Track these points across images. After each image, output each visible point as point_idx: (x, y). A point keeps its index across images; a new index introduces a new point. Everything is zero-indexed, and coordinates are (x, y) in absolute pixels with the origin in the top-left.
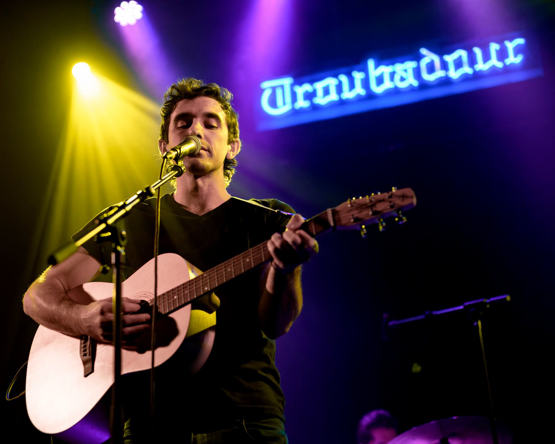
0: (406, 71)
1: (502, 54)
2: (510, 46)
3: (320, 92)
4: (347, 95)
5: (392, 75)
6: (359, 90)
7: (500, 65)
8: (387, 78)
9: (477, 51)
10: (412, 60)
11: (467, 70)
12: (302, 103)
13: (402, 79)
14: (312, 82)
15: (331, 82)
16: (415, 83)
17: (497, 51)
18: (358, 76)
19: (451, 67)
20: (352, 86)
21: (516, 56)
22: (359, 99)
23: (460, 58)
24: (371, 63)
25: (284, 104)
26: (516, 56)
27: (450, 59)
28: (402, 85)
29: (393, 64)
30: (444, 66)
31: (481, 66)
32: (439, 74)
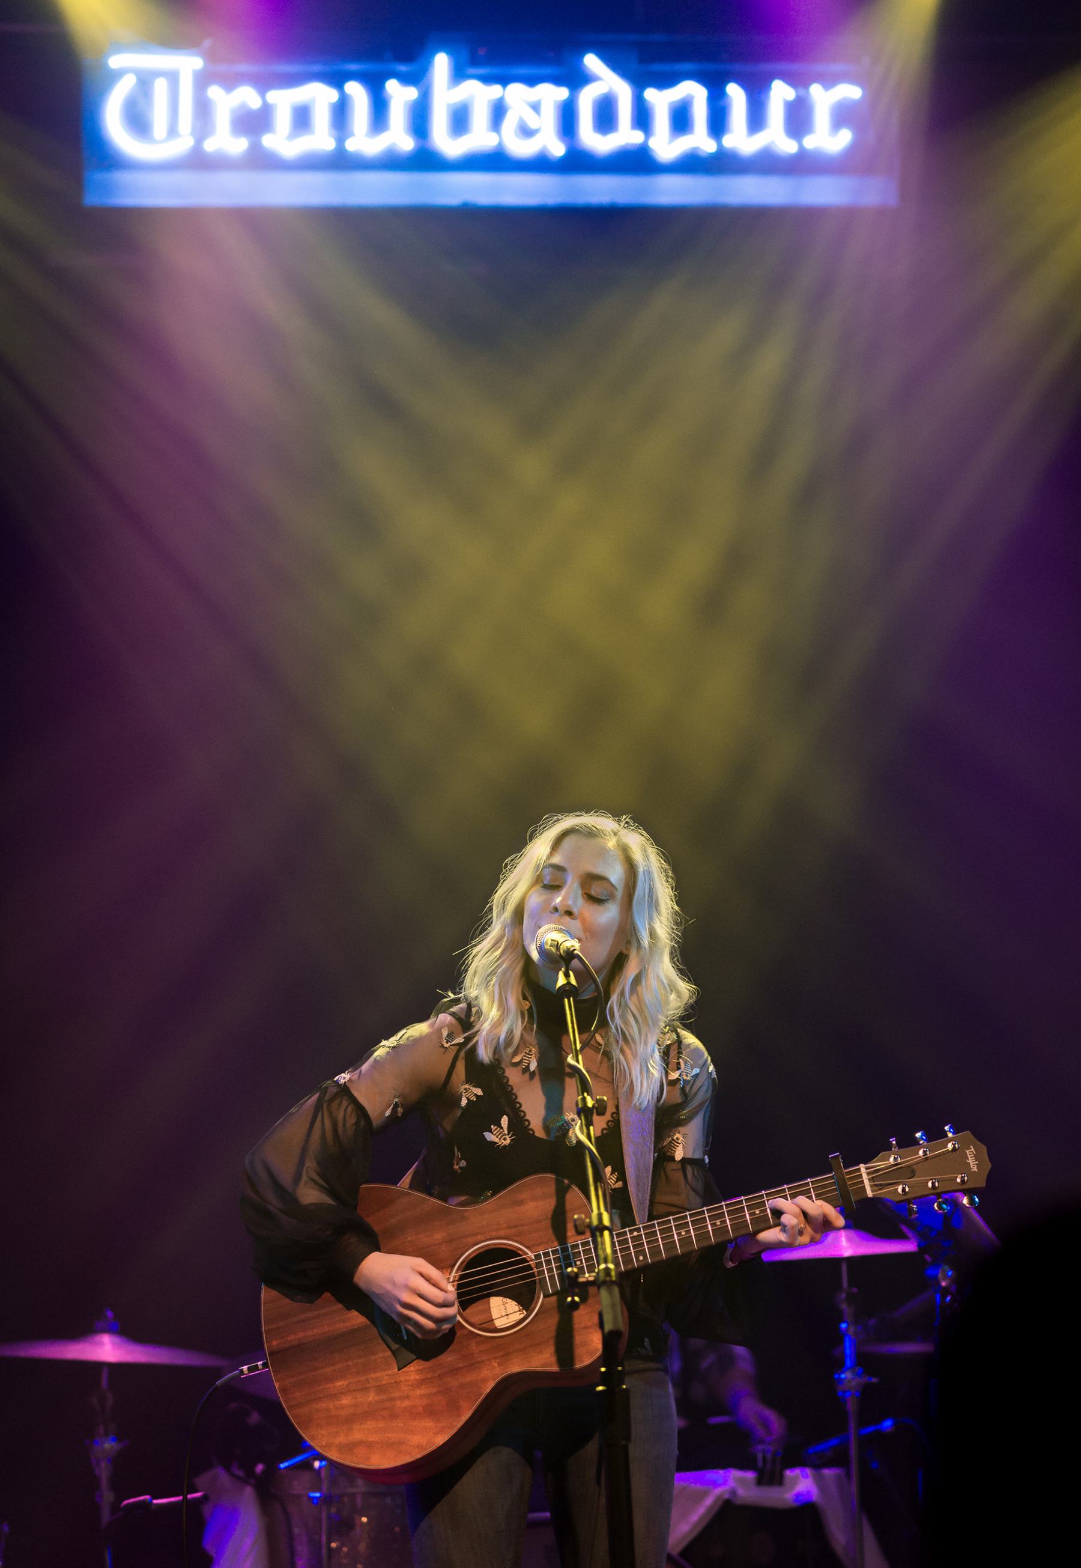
0: (536, 107)
3: (283, 119)
5: (498, 112)
8: (480, 117)
9: (735, 92)
10: (558, 81)
13: (526, 132)
14: (263, 84)
22: (392, 162)
24: (441, 63)
25: (173, 131)
27: (660, 99)
28: (521, 148)
29: (504, 81)
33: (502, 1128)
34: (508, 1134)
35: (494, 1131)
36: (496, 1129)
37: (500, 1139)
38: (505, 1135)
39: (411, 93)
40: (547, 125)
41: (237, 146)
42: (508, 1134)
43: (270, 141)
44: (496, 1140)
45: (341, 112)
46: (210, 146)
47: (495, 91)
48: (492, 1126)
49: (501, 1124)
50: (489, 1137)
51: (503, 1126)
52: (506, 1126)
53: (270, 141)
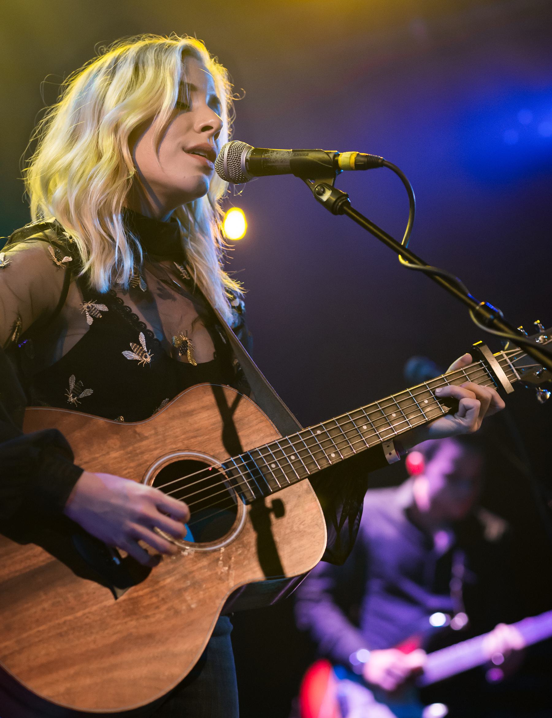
33: (141, 345)
34: (148, 352)
35: (134, 349)
36: (135, 347)
37: (141, 357)
38: (145, 352)
42: (148, 352)
44: (137, 357)
48: (131, 344)
49: (139, 342)
50: (129, 355)
51: (141, 342)
52: (145, 344)
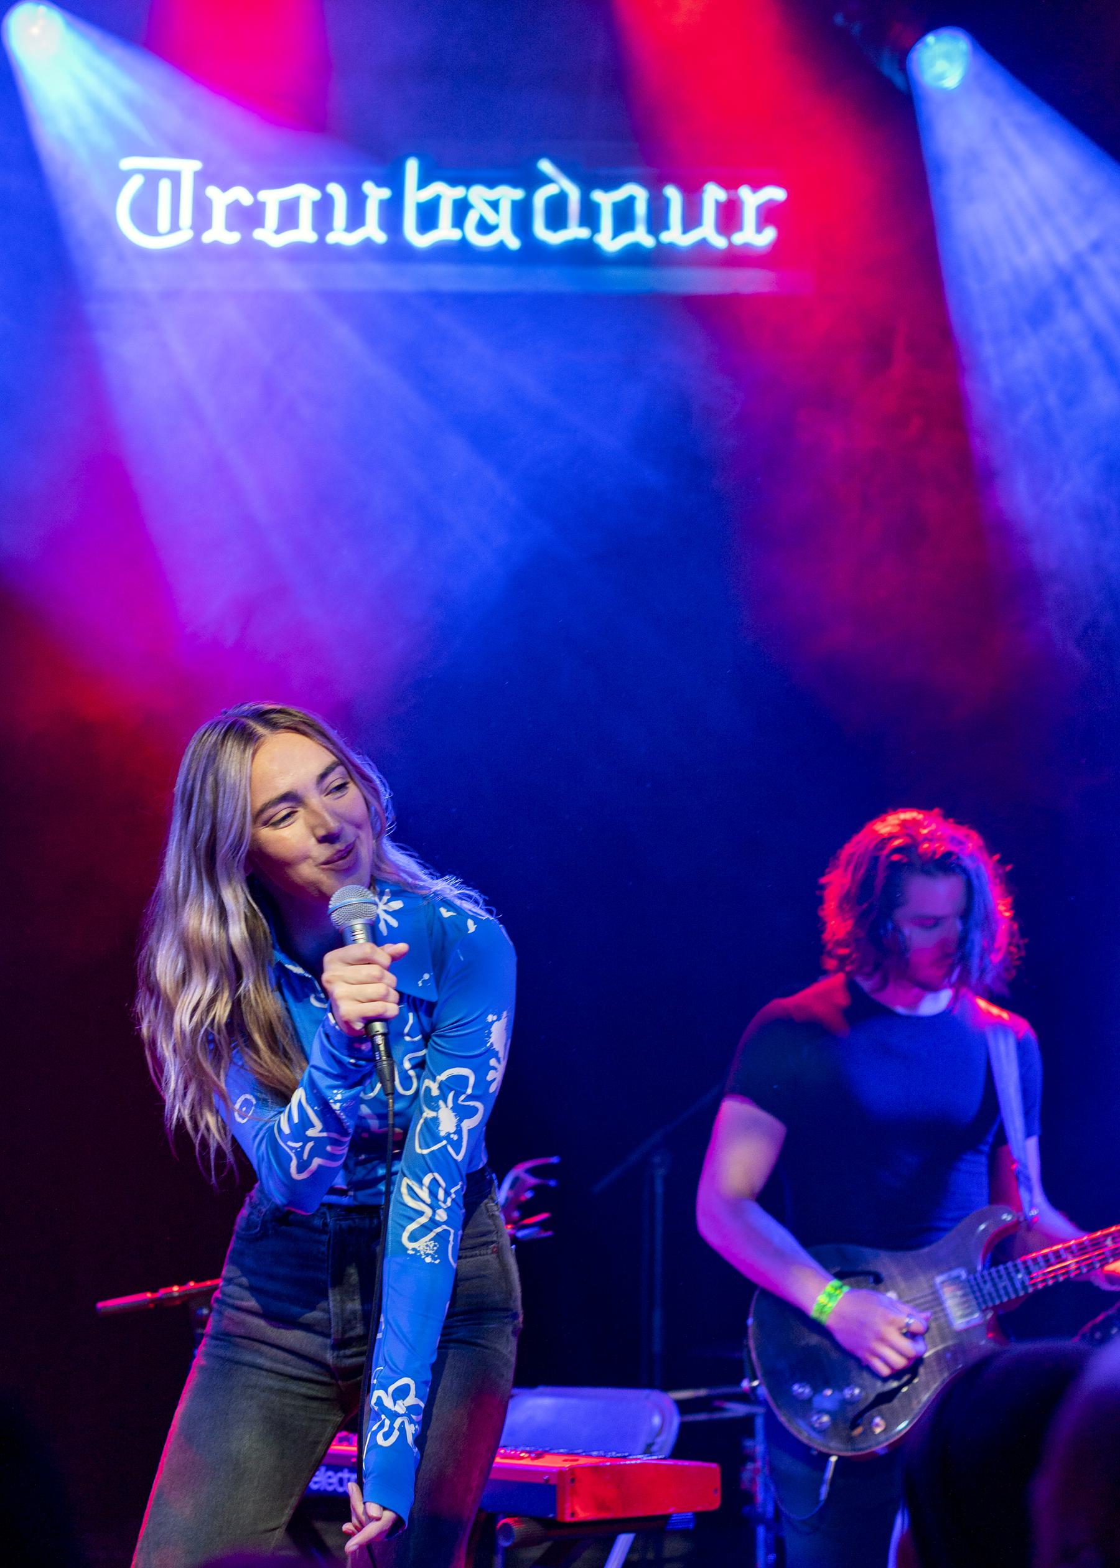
0: (495, 205)
1: (729, 216)
2: (751, 200)
3: (272, 216)
4: (340, 236)
5: (462, 209)
6: (373, 231)
7: (719, 242)
8: (446, 213)
9: (672, 193)
10: (514, 183)
11: (641, 236)
12: (220, 234)
15: (306, 194)
16: (514, 244)
17: (718, 205)
18: (375, 194)
19: (607, 221)
20: (356, 219)
21: (759, 229)
23: (630, 201)
24: (412, 167)
25: (175, 227)
26: (759, 229)
27: (605, 200)
29: (468, 183)
30: (590, 215)
31: (675, 236)
32: (575, 232)
39: (385, 193)
40: (504, 220)
41: (232, 238)
43: (258, 234)
45: (323, 209)
46: (207, 238)
47: (459, 192)
53: (258, 234)
